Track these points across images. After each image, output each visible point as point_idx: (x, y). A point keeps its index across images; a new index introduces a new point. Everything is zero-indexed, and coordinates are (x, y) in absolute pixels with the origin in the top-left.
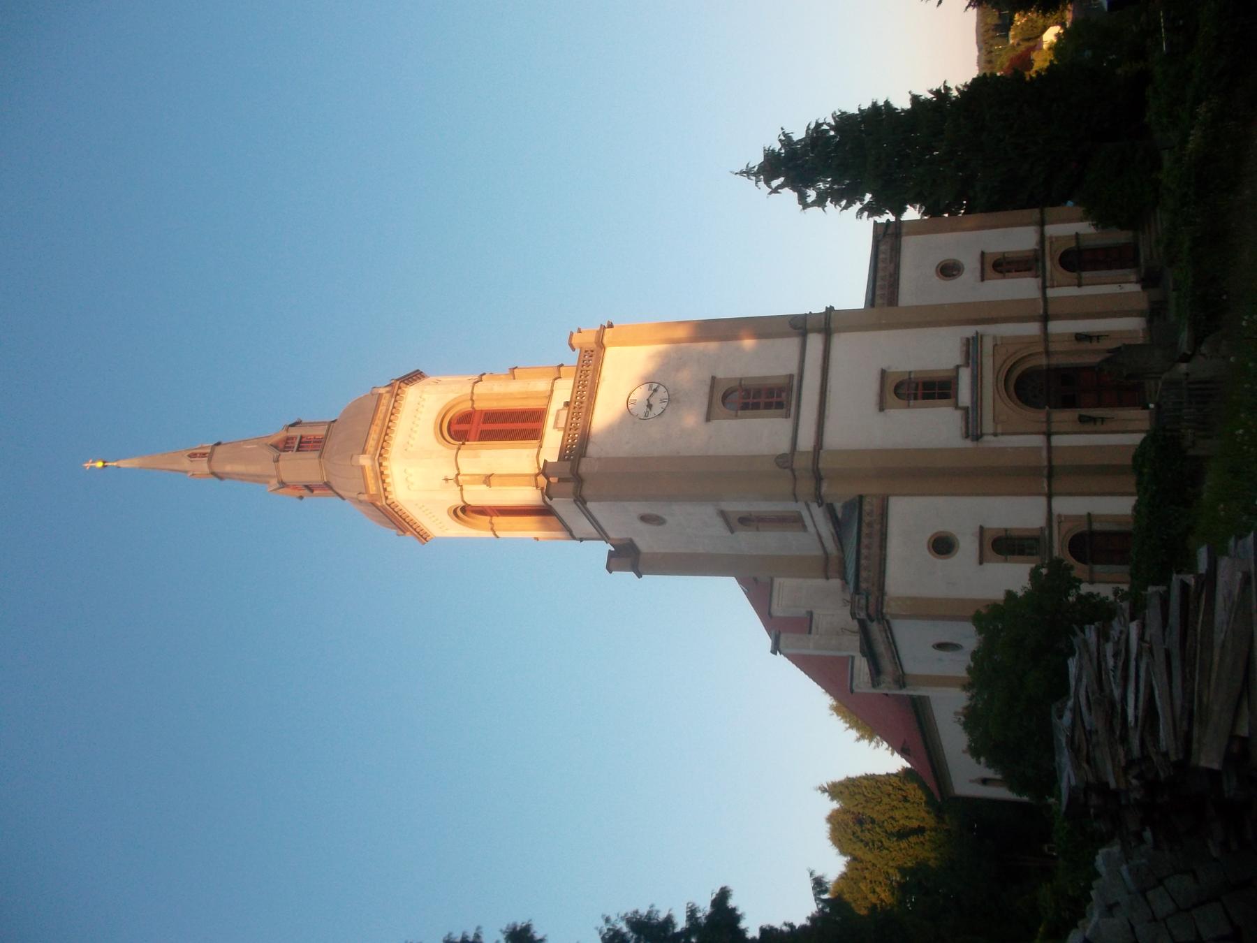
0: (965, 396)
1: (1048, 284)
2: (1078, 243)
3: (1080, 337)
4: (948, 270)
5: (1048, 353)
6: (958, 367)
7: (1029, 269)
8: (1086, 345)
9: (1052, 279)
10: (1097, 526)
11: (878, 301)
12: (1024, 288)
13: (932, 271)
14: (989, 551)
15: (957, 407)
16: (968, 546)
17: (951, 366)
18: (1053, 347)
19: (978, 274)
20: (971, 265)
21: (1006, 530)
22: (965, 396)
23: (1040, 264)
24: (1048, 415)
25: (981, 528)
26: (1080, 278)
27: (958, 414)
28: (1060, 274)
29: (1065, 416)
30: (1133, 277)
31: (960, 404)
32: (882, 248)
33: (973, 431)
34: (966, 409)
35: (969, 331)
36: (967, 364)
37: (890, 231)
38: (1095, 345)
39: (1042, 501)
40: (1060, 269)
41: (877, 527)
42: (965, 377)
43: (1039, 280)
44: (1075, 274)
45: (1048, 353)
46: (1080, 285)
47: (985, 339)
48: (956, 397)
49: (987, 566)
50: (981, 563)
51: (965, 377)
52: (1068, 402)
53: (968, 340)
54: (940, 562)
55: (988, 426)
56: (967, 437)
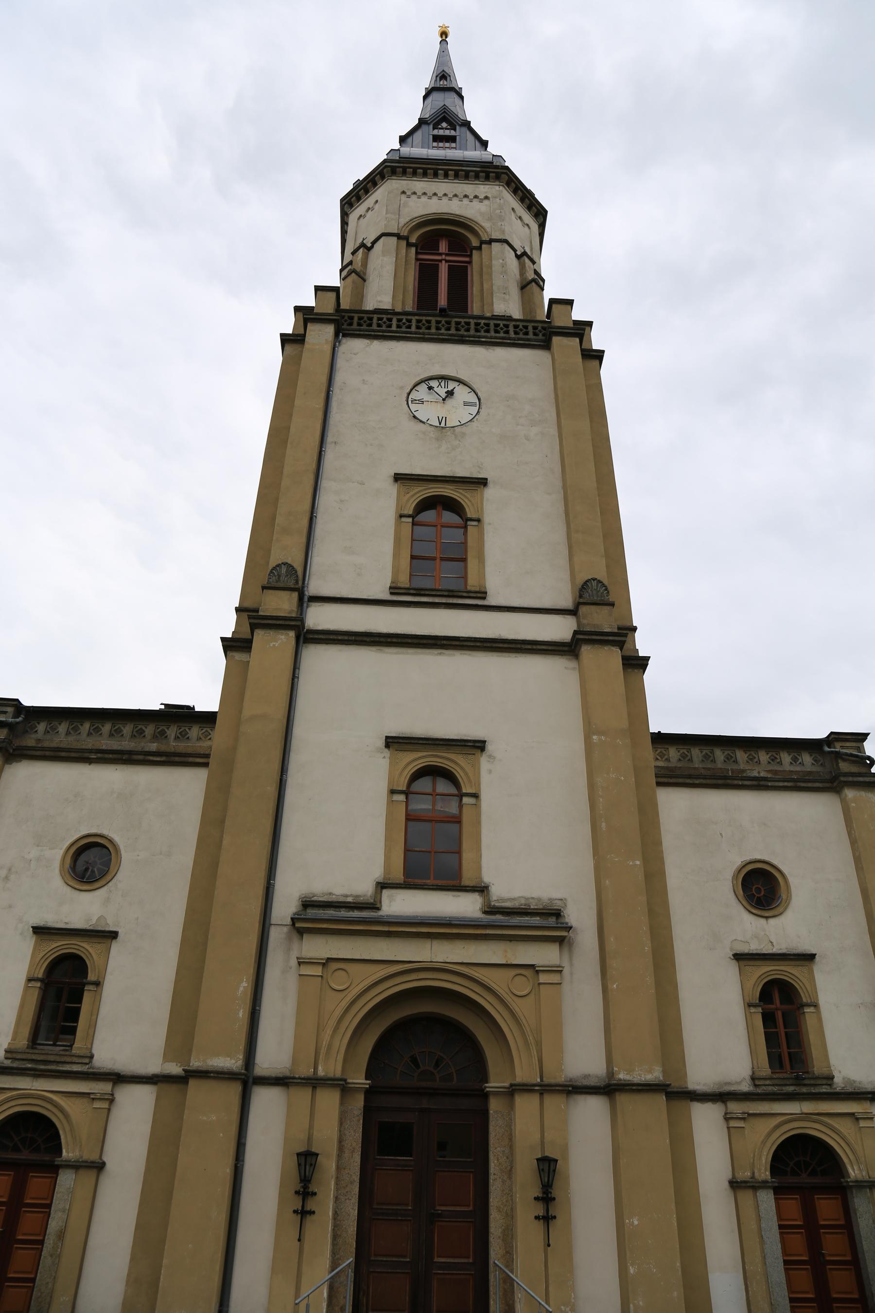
0: (402, 904)
1: (735, 1107)
3: (548, 1168)
4: (761, 887)
5: (514, 1090)
6: (482, 889)
7: (775, 1060)
8: (526, 1183)
9: (748, 1117)
10: (66, 1179)
11: (673, 753)
12: (720, 1043)
14: (57, 947)
15: (382, 886)
16: (81, 909)
17: (487, 878)
18: (525, 1104)
19: (754, 947)
21: (98, 984)
22: (402, 904)
23: (791, 1089)
24: (342, 1086)
25: (113, 935)
27: (364, 888)
28: (763, 1138)
29: (334, 1126)
31: (386, 893)
32: (807, 759)
34: (374, 906)
35: (581, 915)
36: (490, 910)
37: (844, 766)
39: (154, 1066)
40: (778, 1137)
41: (153, 747)
42: (463, 906)
43: (746, 1087)
44: (764, 1173)
45: (514, 1090)
46: (735, 1185)
48: (406, 885)
50: (38, 930)
51: (463, 906)
52: (384, 1138)
55: (319, 947)
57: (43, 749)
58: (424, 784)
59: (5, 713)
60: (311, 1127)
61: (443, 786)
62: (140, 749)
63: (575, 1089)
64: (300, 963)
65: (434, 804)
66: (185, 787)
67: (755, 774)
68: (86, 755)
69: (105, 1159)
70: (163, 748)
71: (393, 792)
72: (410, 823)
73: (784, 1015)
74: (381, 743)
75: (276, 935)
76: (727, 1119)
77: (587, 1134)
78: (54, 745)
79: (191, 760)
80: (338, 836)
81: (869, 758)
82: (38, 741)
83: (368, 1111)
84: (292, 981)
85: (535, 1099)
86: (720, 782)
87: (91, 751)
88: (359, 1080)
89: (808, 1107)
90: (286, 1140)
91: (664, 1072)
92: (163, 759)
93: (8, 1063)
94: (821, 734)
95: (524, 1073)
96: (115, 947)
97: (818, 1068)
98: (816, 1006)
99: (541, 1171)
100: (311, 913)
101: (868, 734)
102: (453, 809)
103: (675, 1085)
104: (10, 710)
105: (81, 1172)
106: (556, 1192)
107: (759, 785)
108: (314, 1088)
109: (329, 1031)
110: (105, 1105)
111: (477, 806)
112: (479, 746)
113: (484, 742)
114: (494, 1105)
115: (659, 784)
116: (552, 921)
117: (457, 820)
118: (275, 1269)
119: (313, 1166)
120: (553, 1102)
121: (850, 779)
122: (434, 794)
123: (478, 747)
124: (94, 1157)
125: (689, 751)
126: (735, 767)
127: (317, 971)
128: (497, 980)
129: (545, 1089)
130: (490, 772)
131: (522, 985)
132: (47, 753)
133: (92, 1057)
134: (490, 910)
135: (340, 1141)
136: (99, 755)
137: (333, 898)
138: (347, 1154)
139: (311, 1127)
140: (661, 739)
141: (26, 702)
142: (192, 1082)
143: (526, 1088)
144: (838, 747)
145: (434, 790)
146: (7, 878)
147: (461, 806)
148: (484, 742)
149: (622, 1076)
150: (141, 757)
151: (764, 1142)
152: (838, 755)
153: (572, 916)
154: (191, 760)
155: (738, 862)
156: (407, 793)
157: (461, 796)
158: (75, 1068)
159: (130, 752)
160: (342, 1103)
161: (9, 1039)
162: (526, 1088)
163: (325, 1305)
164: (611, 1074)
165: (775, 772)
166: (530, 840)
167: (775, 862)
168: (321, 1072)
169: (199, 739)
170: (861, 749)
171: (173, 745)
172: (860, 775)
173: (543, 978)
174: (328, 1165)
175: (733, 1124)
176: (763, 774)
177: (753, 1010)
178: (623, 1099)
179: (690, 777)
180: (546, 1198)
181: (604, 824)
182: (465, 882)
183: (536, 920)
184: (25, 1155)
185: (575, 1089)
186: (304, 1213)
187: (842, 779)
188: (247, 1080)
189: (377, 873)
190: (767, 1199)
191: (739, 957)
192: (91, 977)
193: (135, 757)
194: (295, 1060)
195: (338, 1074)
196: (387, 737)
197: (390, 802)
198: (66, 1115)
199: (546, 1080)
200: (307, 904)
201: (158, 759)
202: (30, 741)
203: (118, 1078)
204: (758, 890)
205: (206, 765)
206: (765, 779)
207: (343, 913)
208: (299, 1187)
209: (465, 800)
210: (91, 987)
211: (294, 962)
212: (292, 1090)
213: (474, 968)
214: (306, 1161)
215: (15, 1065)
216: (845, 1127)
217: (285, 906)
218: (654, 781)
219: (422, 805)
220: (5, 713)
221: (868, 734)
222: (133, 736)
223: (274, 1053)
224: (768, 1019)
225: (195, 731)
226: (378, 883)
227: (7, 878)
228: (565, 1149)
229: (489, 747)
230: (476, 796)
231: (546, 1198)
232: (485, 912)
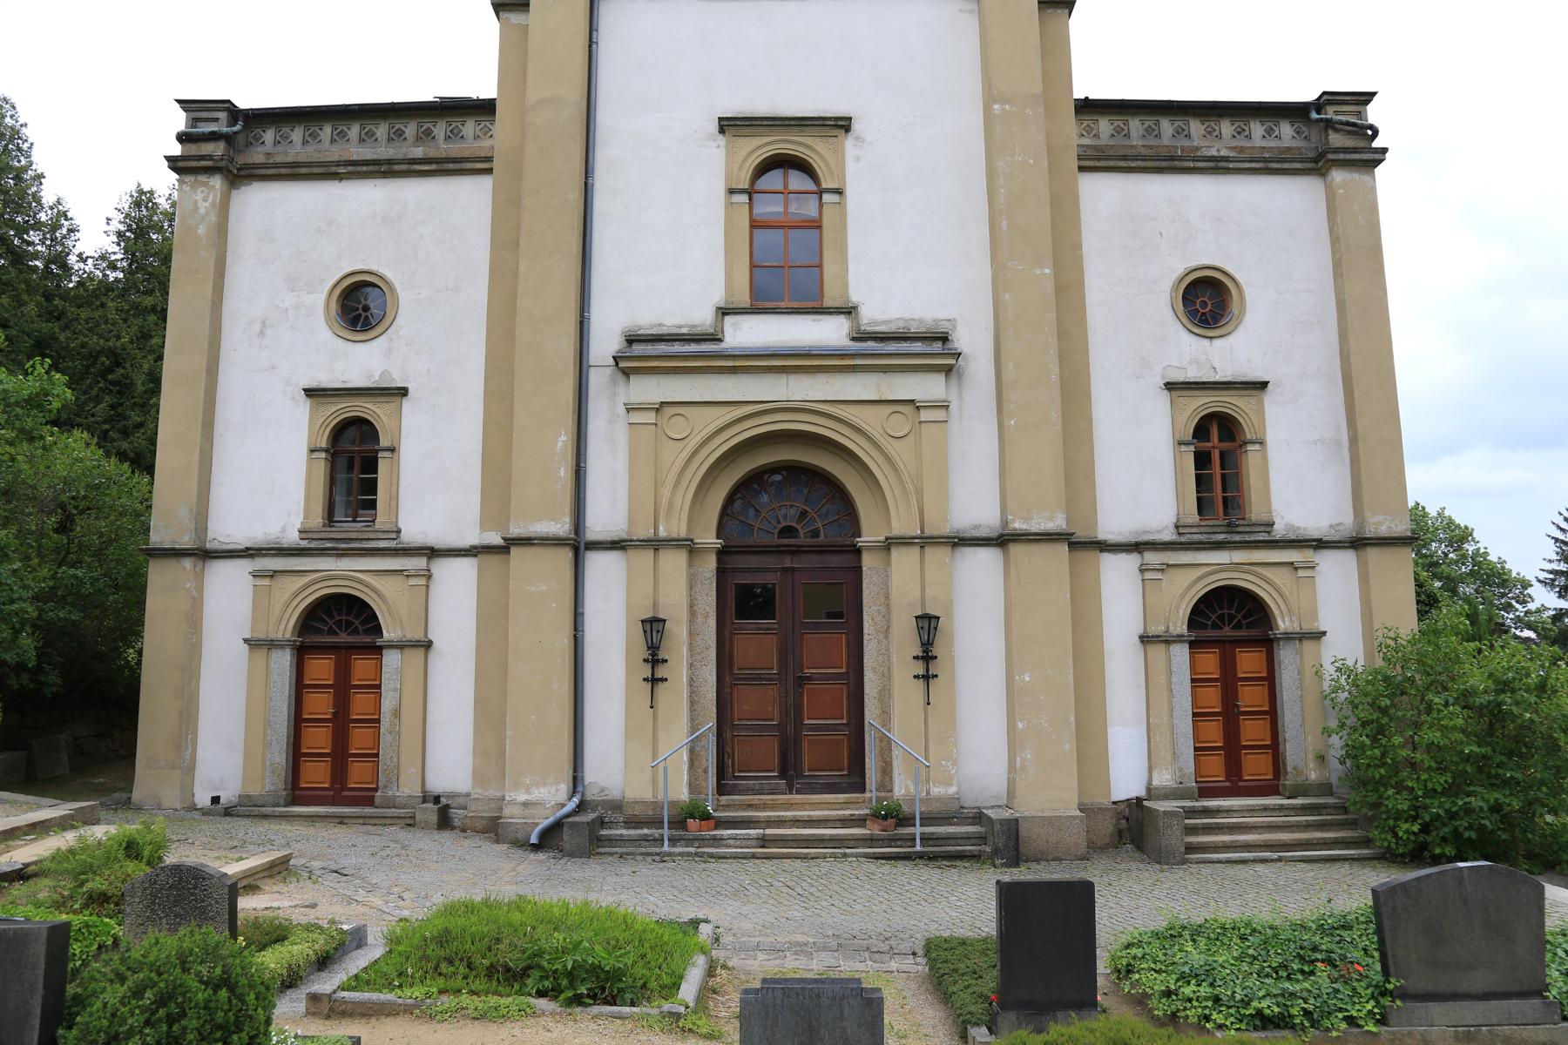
0: (748, 333)
1: (1152, 558)
2: (1289, 637)
3: (928, 625)
4: (1207, 300)
5: (889, 544)
6: (849, 311)
8: (905, 642)
9: (1165, 568)
10: (391, 659)
11: (1104, 125)
13: (1205, 253)
14: (338, 410)
15: (724, 312)
16: (359, 363)
17: (855, 298)
18: (904, 559)
19: (1192, 375)
20: (1226, 356)
22: (748, 333)
23: (1221, 537)
25: (403, 392)
26: (1167, 640)
27: (700, 316)
30: (1164, 779)
32: (1286, 129)
33: (646, 352)
34: (715, 338)
35: (974, 341)
36: (860, 336)
37: (1336, 139)
38: (904, 668)
39: (473, 538)
41: (419, 152)
42: (829, 332)
43: (1168, 535)
44: (1181, 627)
45: (889, 544)
46: (1145, 639)
47: (939, 379)
49: (304, 406)
50: (311, 393)
51: (829, 332)
52: (742, 602)
53: (944, 339)
54: (318, 301)
55: (650, 389)
56: (631, 340)
57: (276, 166)
58: (773, 179)
59: (216, 120)
60: (655, 592)
61: (797, 181)
62: (400, 156)
63: (960, 541)
64: (628, 410)
65: (786, 207)
66: (464, 204)
67: (1213, 152)
68: (333, 169)
69: (431, 637)
70: (432, 153)
71: (731, 191)
72: (756, 231)
73: (1222, 455)
74: (714, 127)
75: (598, 380)
76: (1142, 571)
77: (976, 591)
78: (290, 159)
79: (469, 166)
80: (668, 252)
81: (1371, 127)
82: (268, 155)
83: (722, 573)
84: (621, 433)
85: (916, 550)
86: (1164, 164)
87: (338, 164)
88: (709, 538)
89: (1239, 556)
90: (629, 608)
91: (1068, 520)
92: (433, 167)
93: (304, 544)
94: (1309, 95)
95: (902, 525)
96: (407, 404)
97: (1255, 513)
98: (1261, 443)
99: (920, 629)
100: (638, 349)
101: (1374, 94)
102: (809, 209)
103: (1081, 534)
104: (222, 115)
105: (407, 651)
106: (936, 650)
107: (1217, 166)
108: (656, 550)
109: (669, 486)
110: (423, 581)
111: (841, 205)
112: (843, 125)
113: (850, 119)
114: (868, 562)
115: (1082, 169)
116: (937, 347)
117: (816, 225)
118: (628, 736)
119: (661, 632)
120: (935, 555)
121: (1342, 156)
122: (786, 192)
123: (841, 127)
124: (419, 636)
125: (1126, 123)
126: (1186, 143)
127: (650, 417)
128: (868, 419)
129: (925, 541)
130: (858, 159)
131: (899, 425)
132: (283, 171)
133: (399, 531)
134: (860, 336)
135: (692, 606)
136: (350, 168)
137: (664, 330)
138: (700, 620)
139: (655, 592)
140: (1088, 108)
141: (243, 103)
142: (513, 550)
143: (904, 541)
144: (1330, 113)
145: (786, 186)
146: (262, 333)
147: (821, 206)
148: (850, 119)
149: (1018, 525)
150: (404, 167)
151: (1183, 596)
152: (1329, 124)
153: (963, 340)
154: (469, 166)
155: (1181, 269)
156: (750, 193)
157: (820, 193)
158: (381, 544)
159: (389, 162)
160: (690, 564)
161: (301, 519)
162: (904, 541)
163: (686, 768)
164: (1005, 523)
165: (1241, 150)
166: (909, 246)
167: (1228, 268)
168: (663, 533)
169: (476, 137)
170: (1360, 115)
171: (443, 148)
172: (1355, 150)
173: (925, 415)
174: (678, 631)
175: (1148, 575)
176: (1224, 153)
177: (1184, 448)
178: (1016, 549)
179: (1124, 158)
180: (927, 656)
181: (1004, 223)
182: (828, 302)
183: (917, 347)
184: (343, 638)
185: (960, 541)
186: (654, 681)
187: (1330, 156)
188: (578, 546)
189: (718, 297)
190: (1181, 653)
191: (1170, 386)
192: (384, 442)
193: (397, 167)
194: (631, 521)
195: (683, 534)
196: (720, 119)
197: (729, 205)
198: (380, 595)
199: (928, 532)
200: (631, 340)
201: (427, 168)
202: (256, 156)
203: (433, 553)
204: (1204, 304)
205: (489, 171)
206: (1226, 159)
207: (678, 348)
208: (646, 654)
209: (826, 197)
210: (386, 454)
211: (621, 410)
212: (631, 553)
213: (842, 407)
214: (653, 628)
215: (313, 545)
216: (1281, 577)
217: (605, 343)
218: (1076, 164)
219: (769, 207)
220: (216, 120)
221: (1374, 94)
222: (390, 140)
223: (607, 514)
224: (1202, 460)
225: (470, 127)
226: (719, 309)
227: (262, 333)
228: (949, 606)
229: (855, 125)
230: (839, 192)
231: (927, 656)
232: (854, 339)
